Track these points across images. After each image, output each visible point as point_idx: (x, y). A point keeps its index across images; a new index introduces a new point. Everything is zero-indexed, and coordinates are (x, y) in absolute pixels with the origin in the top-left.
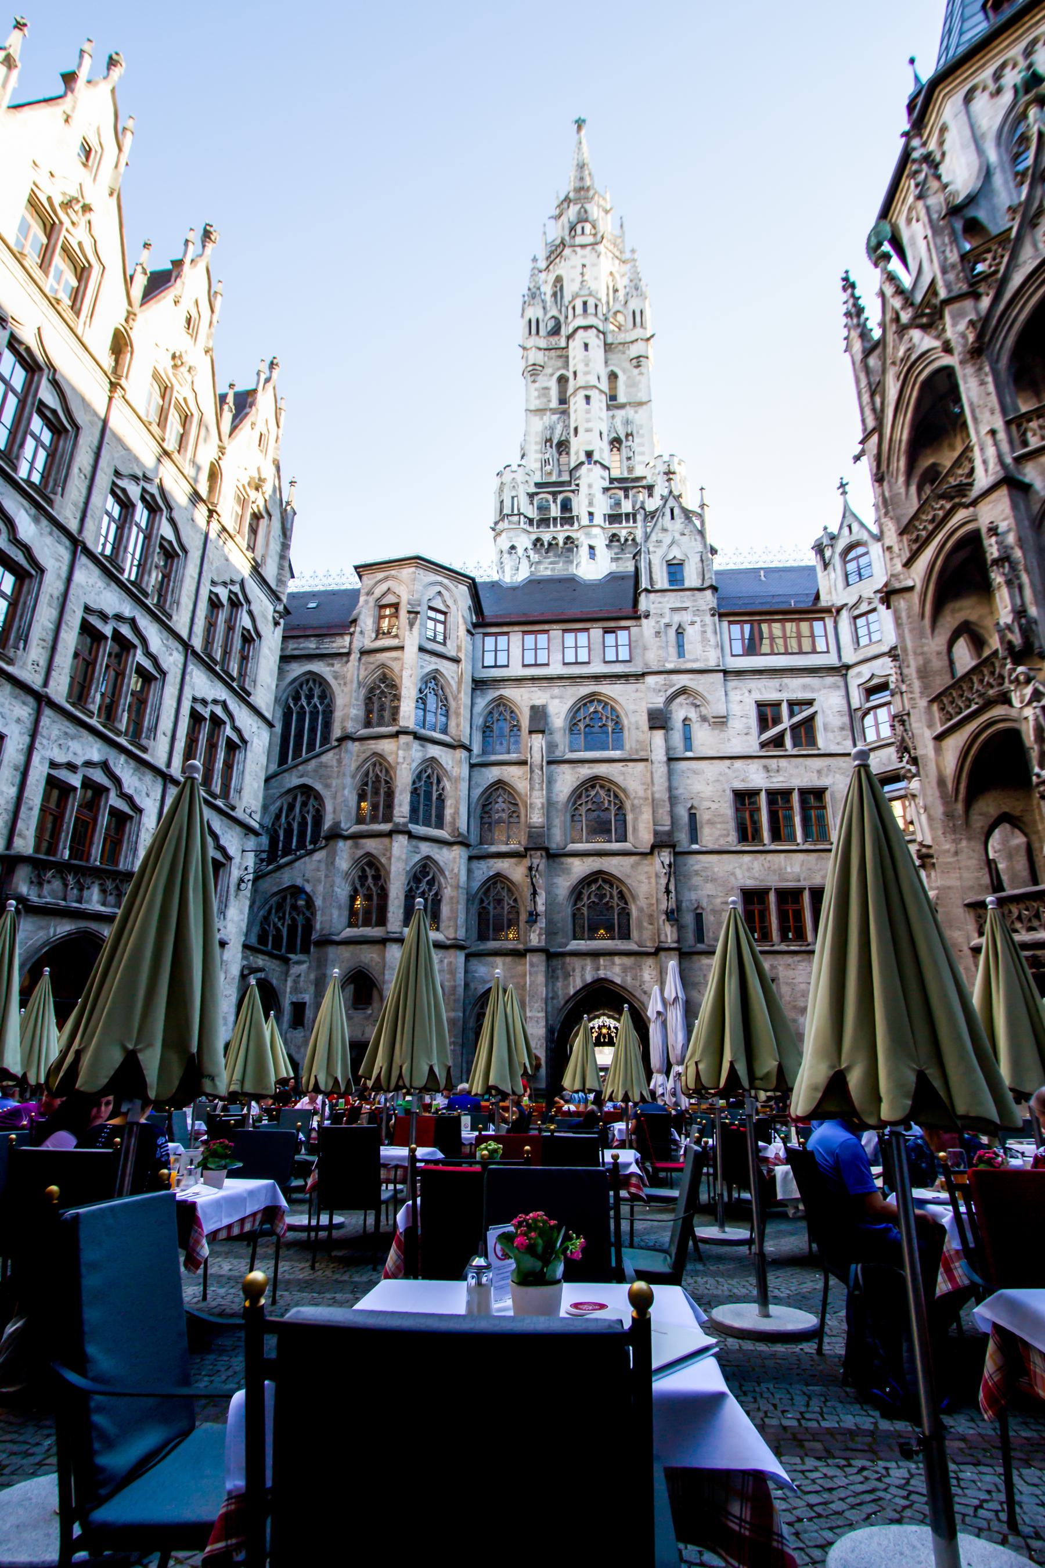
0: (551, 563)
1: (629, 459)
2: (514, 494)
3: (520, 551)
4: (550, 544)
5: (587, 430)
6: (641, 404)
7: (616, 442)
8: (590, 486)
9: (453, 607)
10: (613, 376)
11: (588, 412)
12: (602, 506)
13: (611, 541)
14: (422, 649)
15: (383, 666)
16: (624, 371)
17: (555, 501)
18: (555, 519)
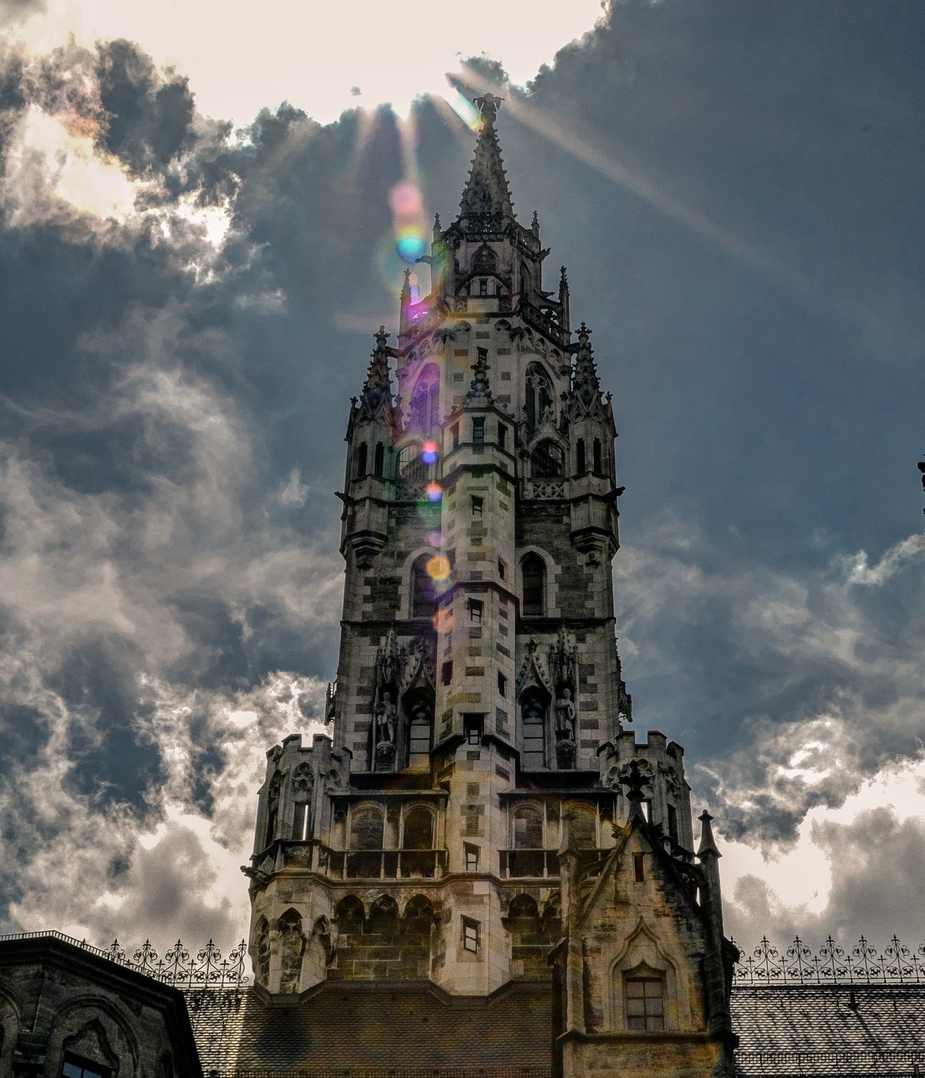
0: (377, 954)
3: (307, 926)
6: (592, 623)
8: (473, 789)
9: (126, 1058)
11: (475, 634)
18: (391, 857)
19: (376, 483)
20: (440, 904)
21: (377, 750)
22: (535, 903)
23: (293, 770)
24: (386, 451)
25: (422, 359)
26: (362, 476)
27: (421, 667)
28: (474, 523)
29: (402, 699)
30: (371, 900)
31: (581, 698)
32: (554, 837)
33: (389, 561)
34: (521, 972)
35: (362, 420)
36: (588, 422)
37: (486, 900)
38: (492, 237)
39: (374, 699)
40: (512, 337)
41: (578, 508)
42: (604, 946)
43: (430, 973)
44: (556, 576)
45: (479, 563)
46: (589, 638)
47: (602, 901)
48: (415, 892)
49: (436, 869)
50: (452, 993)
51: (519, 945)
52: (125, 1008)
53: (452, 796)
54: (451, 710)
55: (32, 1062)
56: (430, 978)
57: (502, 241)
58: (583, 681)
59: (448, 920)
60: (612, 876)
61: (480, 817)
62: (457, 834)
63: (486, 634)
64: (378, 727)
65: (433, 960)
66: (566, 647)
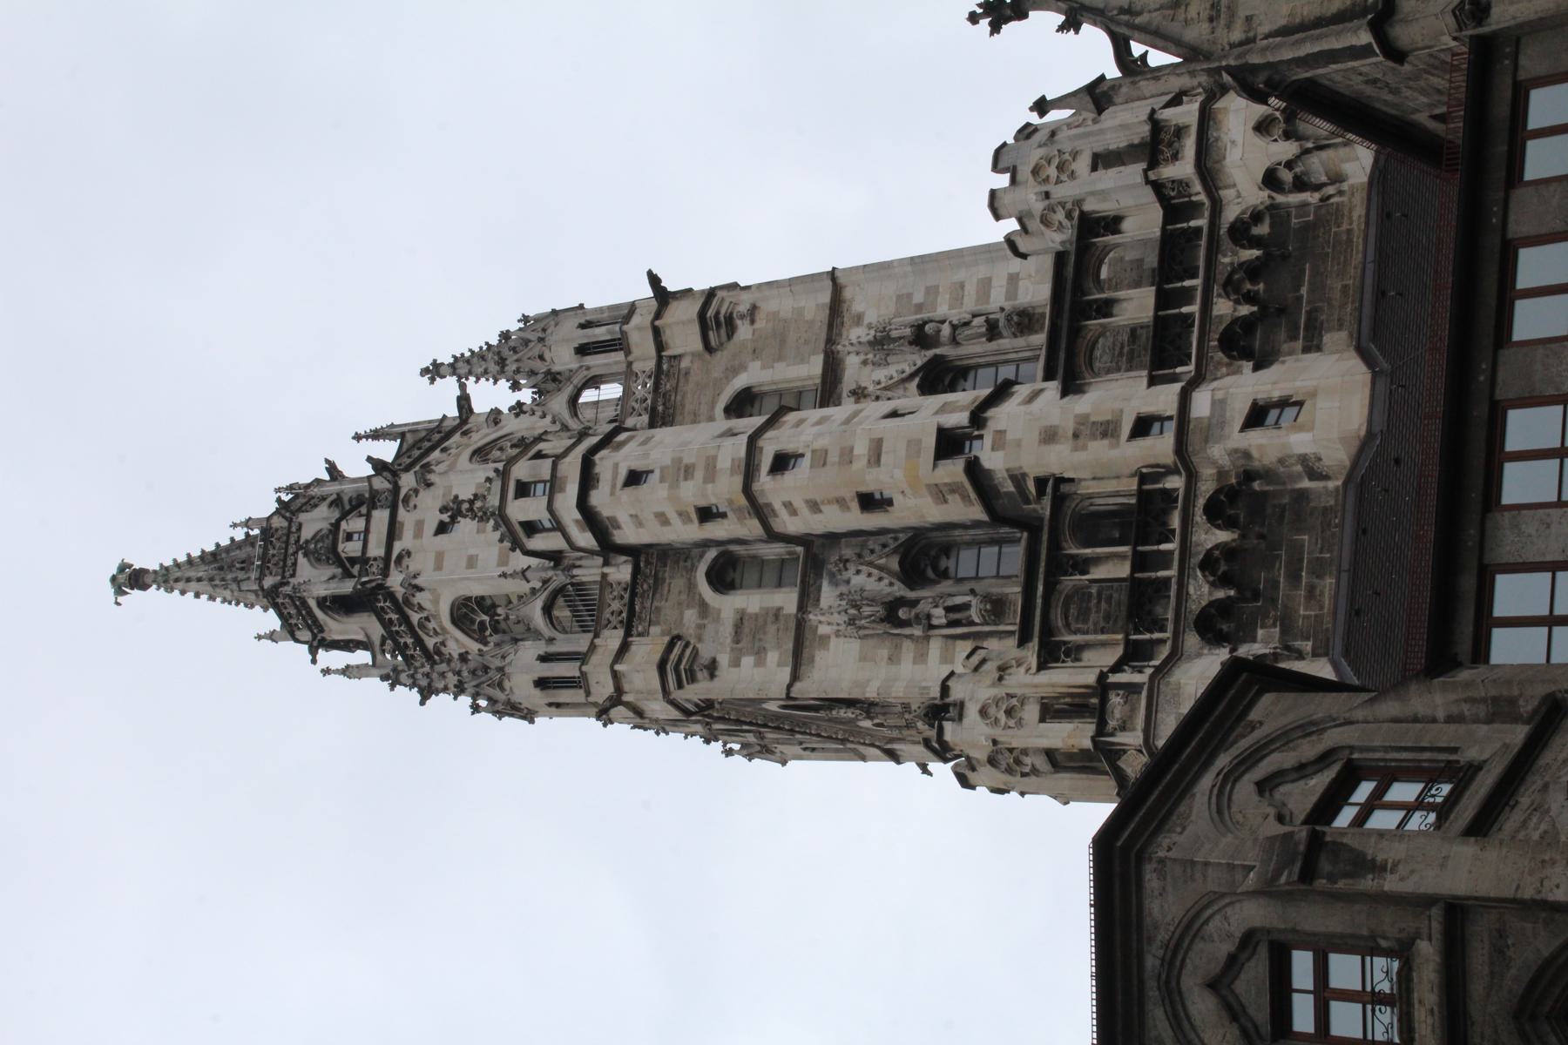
0: (1294, 577)
1: (993, 331)
2: (1031, 712)
4: (1224, 581)
5: (876, 457)
6: (836, 306)
7: (938, 377)
8: (1050, 436)
9: (1333, 738)
10: (742, 403)
11: (821, 458)
12: (1125, 394)
13: (1247, 354)
14: (1479, 828)
15: (1524, 1011)
16: (735, 371)
18: (1140, 562)
19: (595, 659)
20: (1221, 474)
21: (986, 623)
22: (1235, 321)
24: (553, 649)
25: (443, 629)
27: (870, 564)
28: (662, 480)
29: (912, 589)
30: (1206, 588)
31: (943, 309)
32: (1137, 306)
33: (710, 628)
34: (1344, 335)
35: (502, 689)
36: (550, 340)
37: (1220, 395)
38: (292, 540)
39: (907, 636)
40: (429, 485)
41: (670, 342)
42: (1242, 13)
43: (1331, 485)
44: (763, 367)
45: (719, 465)
46: (858, 307)
47: (1174, 28)
48: (1199, 517)
49: (1168, 485)
50: (1363, 432)
51: (1299, 344)
52: (1243, 744)
53: (1056, 470)
54: (928, 486)
55: (1302, 848)
56: (1339, 483)
57: (300, 525)
58: (919, 308)
59: (1247, 455)
60: (1138, 20)
61: (1093, 419)
62: (1114, 453)
63: (820, 443)
64: (952, 624)
65: (1311, 479)
66: (864, 339)
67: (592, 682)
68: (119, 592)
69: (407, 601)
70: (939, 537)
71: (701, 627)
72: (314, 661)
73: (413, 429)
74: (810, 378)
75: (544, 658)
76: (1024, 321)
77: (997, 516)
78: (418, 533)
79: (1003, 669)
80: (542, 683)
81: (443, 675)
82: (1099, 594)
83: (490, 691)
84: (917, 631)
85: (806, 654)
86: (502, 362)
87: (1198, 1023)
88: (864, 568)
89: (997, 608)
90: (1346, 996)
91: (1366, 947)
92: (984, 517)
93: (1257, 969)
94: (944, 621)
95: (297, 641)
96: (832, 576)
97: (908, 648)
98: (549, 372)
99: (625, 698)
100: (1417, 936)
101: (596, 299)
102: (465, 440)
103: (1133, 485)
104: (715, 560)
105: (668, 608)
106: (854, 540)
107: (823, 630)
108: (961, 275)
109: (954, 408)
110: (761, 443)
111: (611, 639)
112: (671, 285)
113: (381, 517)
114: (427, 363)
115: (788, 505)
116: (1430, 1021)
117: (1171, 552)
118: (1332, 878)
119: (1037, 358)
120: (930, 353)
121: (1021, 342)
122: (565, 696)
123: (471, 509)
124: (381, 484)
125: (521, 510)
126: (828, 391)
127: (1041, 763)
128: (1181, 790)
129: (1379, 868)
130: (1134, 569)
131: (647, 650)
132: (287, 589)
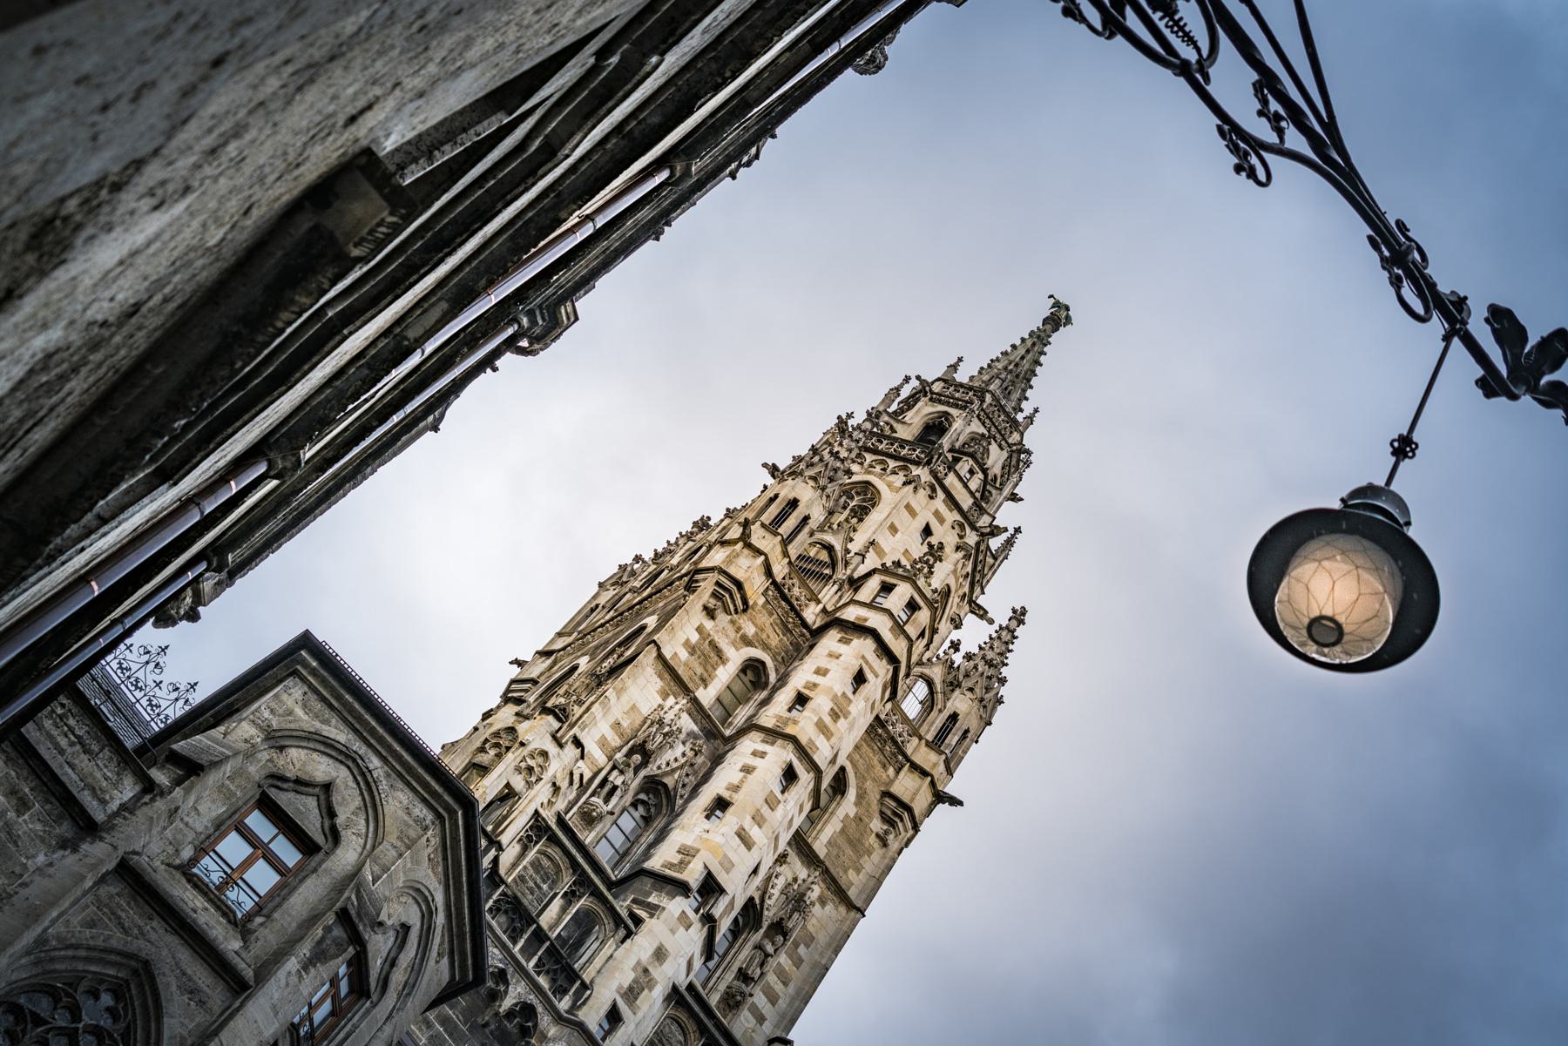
2: (518, 783)
8: (660, 954)
9: (391, 999)
11: (771, 802)
15: (144, 971)
16: (861, 797)
17: (570, 897)
18: (540, 936)
19: (779, 549)
23: (530, 748)
24: (806, 530)
26: (773, 527)
27: (682, 767)
31: (783, 959)
33: (732, 634)
40: (958, 548)
48: (532, 999)
49: (567, 998)
58: (796, 945)
62: (614, 986)
63: (780, 809)
64: (605, 780)
67: (767, 535)
68: (1057, 304)
69: (905, 468)
70: (659, 823)
71: (739, 629)
72: (918, 378)
73: (993, 569)
74: (816, 838)
75: (806, 519)
76: (733, 1001)
77: (640, 873)
78: (937, 514)
79: (556, 789)
80: (793, 504)
81: (850, 451)
82: (539, 888)
83: (817, 470)
84: (619, 756)
85: (666, 676)
86: (990, 664)
87: (315, 755)
88: (683, 760)
89: (589, 819)
90: (248, 863)
91: (266, 906)
92: (648, 865)
93: (312, 823)
94: (611, 779)
95: (939, 379)
96: (696, 737)
97: (615, 741)
98: (959, 685)
99: (740, 544)
100: (246, 947)
101: (974, 756)
102: (961, 593)
103: (586, 977)
104: (767, 676)
105: (765, 620)
106: (704, 770)
107: (671, 700)
108: (791, 989)
109: (725, 911)
110: (812, 775)
111: (780, 570)
112: (943, 808)
113: (966, 502)
114: (1027, 618)
115: (763, 755)
116: (191, 904)
117: (528, 961)
118: (328, 929)
119: (704, 986)
120: (765, 925)
121: (722, 987)
122: (774, 510)
123: (927, 562)
124: (984, 521)
125: (903, 591)
126: (800, 842)
127: (484, 759)
128: (450, 881)
129: (307, 965)
130: (539, 927)
131: (756, 586)
132: (975, 406)
